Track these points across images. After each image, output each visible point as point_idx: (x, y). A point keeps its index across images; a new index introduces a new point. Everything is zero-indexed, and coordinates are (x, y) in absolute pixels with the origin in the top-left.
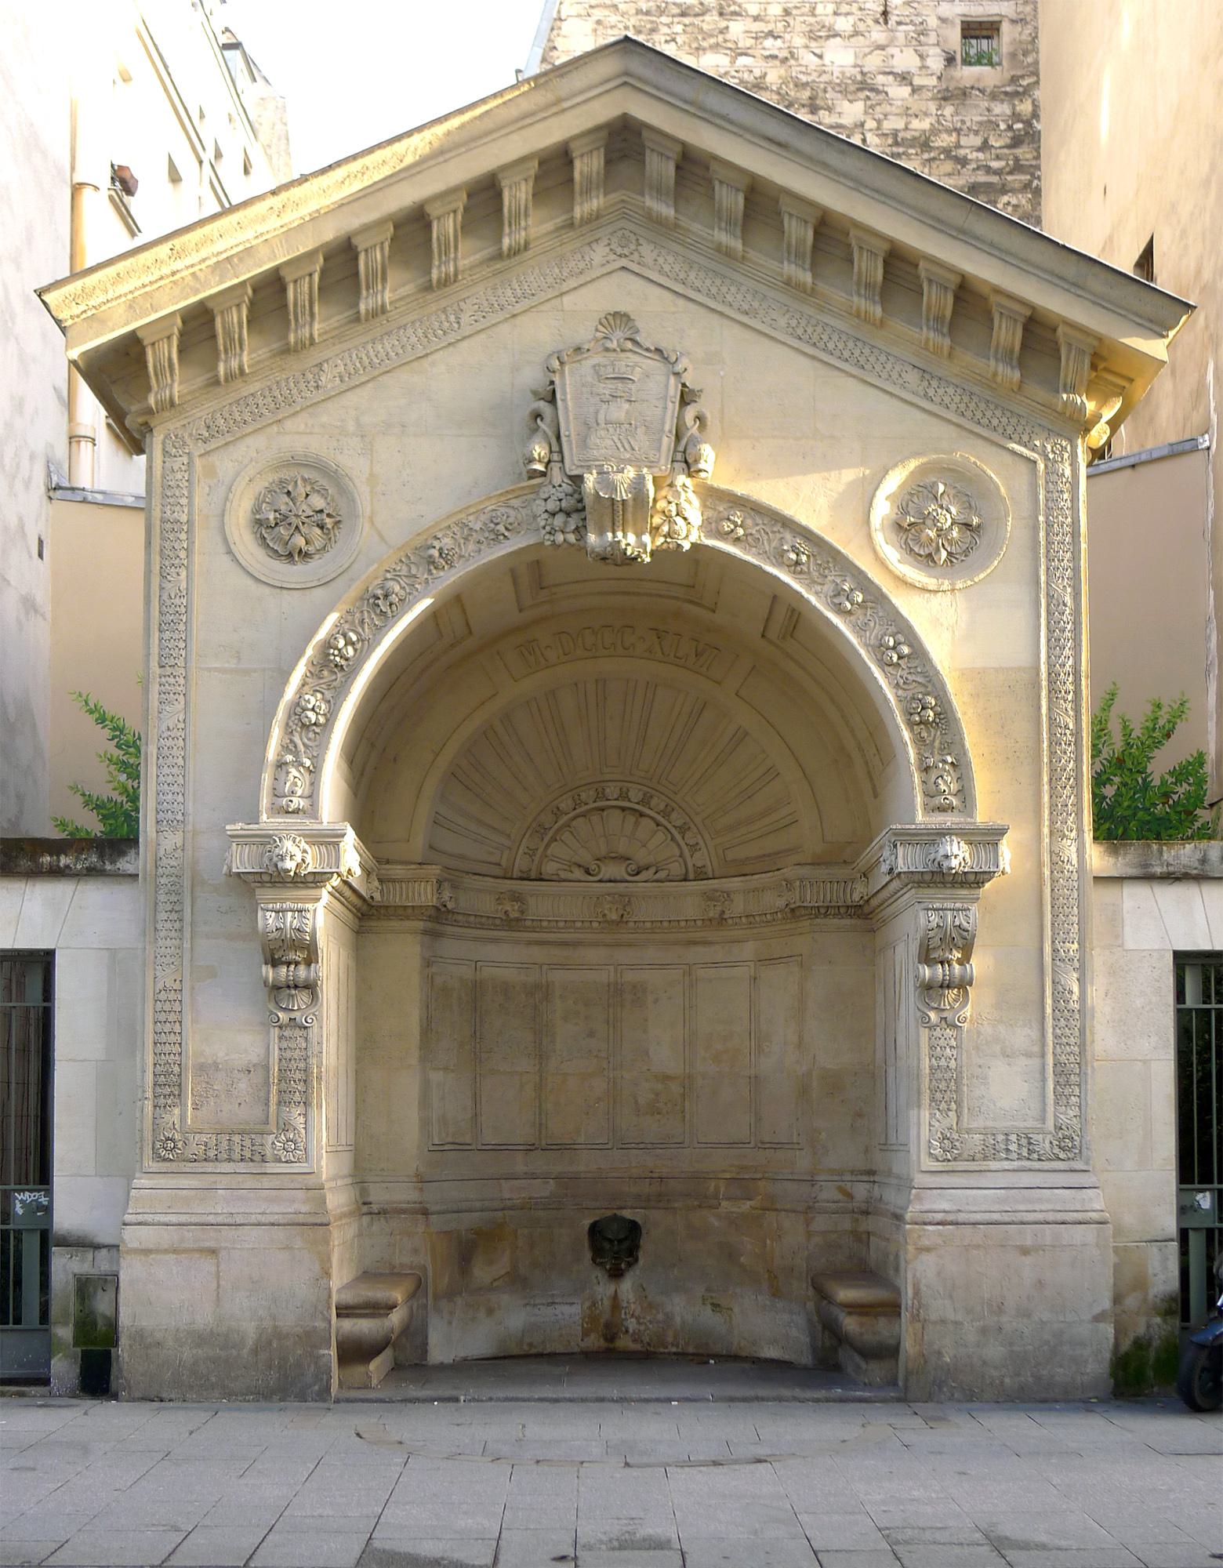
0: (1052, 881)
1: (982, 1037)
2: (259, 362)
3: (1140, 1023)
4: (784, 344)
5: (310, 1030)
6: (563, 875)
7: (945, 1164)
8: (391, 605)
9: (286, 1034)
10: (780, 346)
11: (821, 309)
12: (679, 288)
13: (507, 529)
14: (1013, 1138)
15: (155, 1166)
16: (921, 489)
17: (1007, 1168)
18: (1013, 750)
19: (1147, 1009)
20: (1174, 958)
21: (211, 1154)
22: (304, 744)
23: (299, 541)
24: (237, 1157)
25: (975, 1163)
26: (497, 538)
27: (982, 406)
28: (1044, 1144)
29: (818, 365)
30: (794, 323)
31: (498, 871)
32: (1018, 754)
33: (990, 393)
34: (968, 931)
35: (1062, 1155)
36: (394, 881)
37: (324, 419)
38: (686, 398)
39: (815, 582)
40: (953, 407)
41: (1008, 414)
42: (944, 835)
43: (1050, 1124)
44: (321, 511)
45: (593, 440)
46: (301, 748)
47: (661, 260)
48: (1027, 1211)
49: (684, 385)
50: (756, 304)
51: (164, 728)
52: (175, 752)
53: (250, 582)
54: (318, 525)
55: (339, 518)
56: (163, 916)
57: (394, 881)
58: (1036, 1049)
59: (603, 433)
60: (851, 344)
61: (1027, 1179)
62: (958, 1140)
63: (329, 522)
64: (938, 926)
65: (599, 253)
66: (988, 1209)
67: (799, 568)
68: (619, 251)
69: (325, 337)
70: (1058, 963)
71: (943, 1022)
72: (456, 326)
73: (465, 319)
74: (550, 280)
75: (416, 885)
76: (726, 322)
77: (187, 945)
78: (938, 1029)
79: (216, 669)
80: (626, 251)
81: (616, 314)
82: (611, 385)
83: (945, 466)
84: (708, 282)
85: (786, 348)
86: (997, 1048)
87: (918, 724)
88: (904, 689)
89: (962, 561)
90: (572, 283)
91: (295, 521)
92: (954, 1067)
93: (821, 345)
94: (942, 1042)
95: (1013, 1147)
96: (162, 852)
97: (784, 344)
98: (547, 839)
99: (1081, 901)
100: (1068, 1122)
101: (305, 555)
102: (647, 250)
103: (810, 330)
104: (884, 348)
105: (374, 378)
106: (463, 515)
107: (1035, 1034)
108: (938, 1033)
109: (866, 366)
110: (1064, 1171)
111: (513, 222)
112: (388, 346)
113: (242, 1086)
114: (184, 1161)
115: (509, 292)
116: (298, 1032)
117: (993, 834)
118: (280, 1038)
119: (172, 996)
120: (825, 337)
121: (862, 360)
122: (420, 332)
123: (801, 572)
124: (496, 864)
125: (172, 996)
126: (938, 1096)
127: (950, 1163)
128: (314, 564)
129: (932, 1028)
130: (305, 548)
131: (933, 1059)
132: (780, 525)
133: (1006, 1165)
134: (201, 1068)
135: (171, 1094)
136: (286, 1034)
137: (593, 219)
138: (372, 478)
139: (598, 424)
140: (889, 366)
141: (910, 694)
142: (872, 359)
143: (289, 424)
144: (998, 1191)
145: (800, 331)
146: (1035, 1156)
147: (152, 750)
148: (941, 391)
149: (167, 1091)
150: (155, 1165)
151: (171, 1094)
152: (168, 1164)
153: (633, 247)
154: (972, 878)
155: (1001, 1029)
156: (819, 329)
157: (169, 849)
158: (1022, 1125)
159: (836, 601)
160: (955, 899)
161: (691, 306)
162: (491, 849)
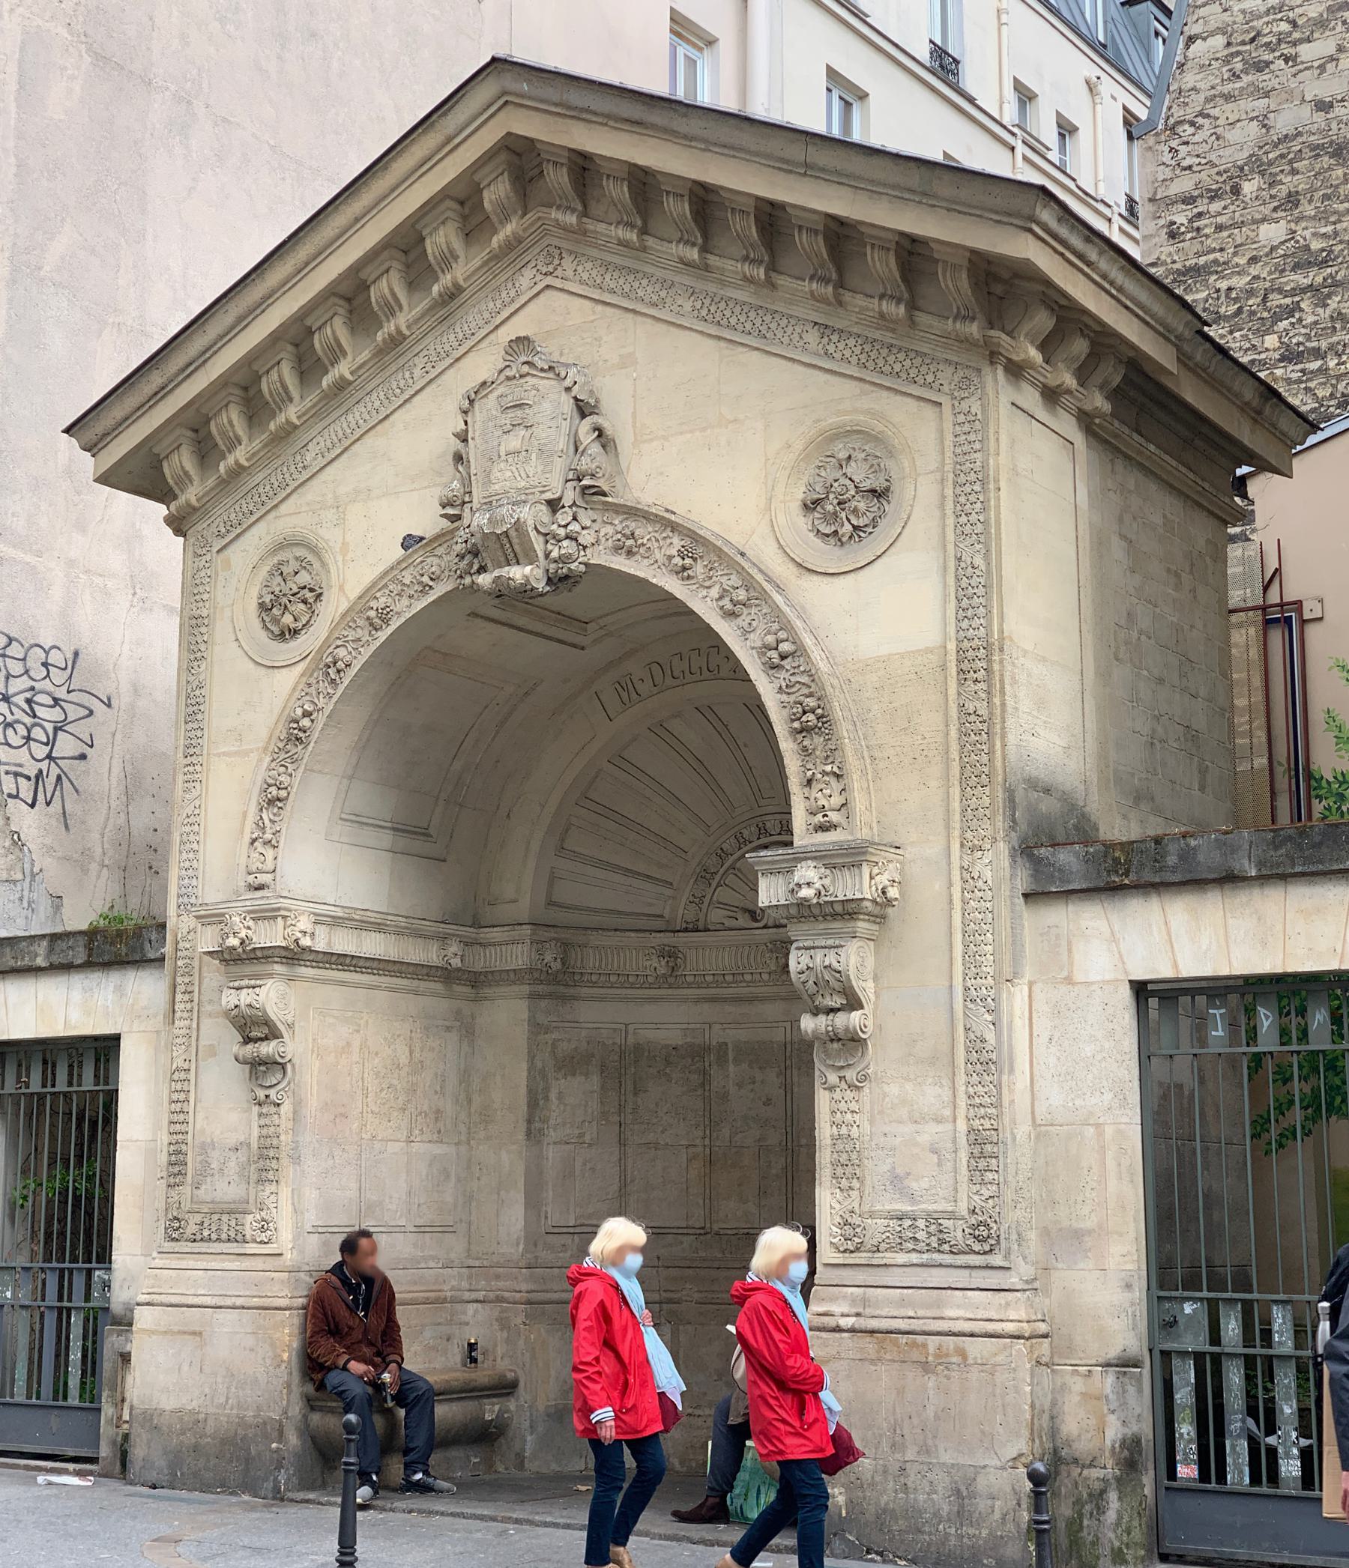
0: (965, 902)
1: (887, 1100)
2: (254, 455)
3: (1090, 1076)
4: (691, 329)
5: (282, 1107)
6: (729, 923)
7: (847, 1255)
8: (339, 671)
9: (264, 1110)
10: (687, 333)
11: (723, 283)
13: (432, 579)
14: (921, 1223)
15: (169, 1246)
16: (829, 459)
17: (915, 1261)
18: (921, 747)
19: (1099, 1057)
20: (96, 1038)
21: (206, 1233)
22: (270, 820)
23: (287, 619)
24: (224, 1236)
25: (880, 1255)
26: (425, 589)
27: (884, 352)
28: (958, 1233)
29: (723, 344)
30: (698, 304)
31: (658, 924)
32: (925, 753)
33: (891, 335)
34: (839, 972)
35: (977, 1247)
36: (494, 944)
38: (583, 409)
39: (702, 586)
40: (854, 360)
41: (912, 355)
42: (806, 859)
43: (963, 1208)
44: (305, 587)
45: (496, 474)
46: (267, 822)
47: (580, 269)
48: (934, 1318)
49: (576, 399)
50: (663, 294)
51: (185, 815)
52: (192, 837)
53: (251, 665)
54: (303, 601)
55: (320, 591)
56: (179, 997)
57: (494, 944)
58: (948, 1112)
59: (502, 465)
60: (752, 315)
61: (937, 1277)
62: (860, 1226)
63: (309, 595)
64: (808, 968)
65: (526, 278)
66: (890, 1314)
67: (685, 574)
68: (544, 270)
69: (305, 418)
70: (971, 1006)
71: (843, 1082)
72: (411, 381)
73: (417, 372)
74: (486, 315)
75: (520, 946)
76: (640, 319)
77: (194, 1026)
78: (838, 1090)
79: (224, 754)
80: (550, 268)
81: (518, 338)
82: (511, 414)
83: (849, 428)
84: (621, 281)
85: (693, 334)
87: (801, 732)
88: (789, 694)
89: (871, 533)
90: (505, 314)
91: (284, 600)
92: (856, 1136)
93: (724, 322)
94: (843, 1106)
95: (921, 1235)
96: (180, 936)
97: (691, 329)
98: (714, 884)
99: (996, 926)
100: (983, 1204)
101: (295, 633)
102: (568, 263)
103: (713, 309)
104: (785, 311)
105: (346, 449)
106: (396, 572)
107: (946, 1094)
108: (837, 1095)
109: (768, 335)
110: (980, 1267)
111: (444, 266)
112: (357, 414)
113: (232, 1164)
114: (186, 1240)
115: (452, 337)
116: (273, 1109)
117: (853, 854)
118: (260, 1115)
119: (183, 1075)
120: (728, 313)
121: (763, 329)
122: (382, 397)
123: (689, 577)
124: (659, 916)
125: (183, 1075)
126: (840, 1171)
127: (853, 1255)
128: (302, 638)
129: (831, 1089)
130: (292, 626)
131: (834, 1127)
132: (669, 529)
133: (915, 1258)
135: (180, 1173)
136: (264, 1110)
137: (511, 246)
139: (499, 456)
140: (789, 330)
141: (792, 698)
142: (773, 326)
143: (284, 508)
144: (905, 1291)
145: (704, 312)
146: (946, 1247)
147: (176, 837)
148: (841, 346)
149: (176, 1169)
150: (166, 1244)
151: (180, 1173)
152: (173, 1244)
153: (556, 262)
154: (838, 908)
156: (722, 305)
157: (185, 931)
158: (931, 1207)
159: (721, 603)
160: (827, 934)
161: (609, 310)
162: (649, 900)
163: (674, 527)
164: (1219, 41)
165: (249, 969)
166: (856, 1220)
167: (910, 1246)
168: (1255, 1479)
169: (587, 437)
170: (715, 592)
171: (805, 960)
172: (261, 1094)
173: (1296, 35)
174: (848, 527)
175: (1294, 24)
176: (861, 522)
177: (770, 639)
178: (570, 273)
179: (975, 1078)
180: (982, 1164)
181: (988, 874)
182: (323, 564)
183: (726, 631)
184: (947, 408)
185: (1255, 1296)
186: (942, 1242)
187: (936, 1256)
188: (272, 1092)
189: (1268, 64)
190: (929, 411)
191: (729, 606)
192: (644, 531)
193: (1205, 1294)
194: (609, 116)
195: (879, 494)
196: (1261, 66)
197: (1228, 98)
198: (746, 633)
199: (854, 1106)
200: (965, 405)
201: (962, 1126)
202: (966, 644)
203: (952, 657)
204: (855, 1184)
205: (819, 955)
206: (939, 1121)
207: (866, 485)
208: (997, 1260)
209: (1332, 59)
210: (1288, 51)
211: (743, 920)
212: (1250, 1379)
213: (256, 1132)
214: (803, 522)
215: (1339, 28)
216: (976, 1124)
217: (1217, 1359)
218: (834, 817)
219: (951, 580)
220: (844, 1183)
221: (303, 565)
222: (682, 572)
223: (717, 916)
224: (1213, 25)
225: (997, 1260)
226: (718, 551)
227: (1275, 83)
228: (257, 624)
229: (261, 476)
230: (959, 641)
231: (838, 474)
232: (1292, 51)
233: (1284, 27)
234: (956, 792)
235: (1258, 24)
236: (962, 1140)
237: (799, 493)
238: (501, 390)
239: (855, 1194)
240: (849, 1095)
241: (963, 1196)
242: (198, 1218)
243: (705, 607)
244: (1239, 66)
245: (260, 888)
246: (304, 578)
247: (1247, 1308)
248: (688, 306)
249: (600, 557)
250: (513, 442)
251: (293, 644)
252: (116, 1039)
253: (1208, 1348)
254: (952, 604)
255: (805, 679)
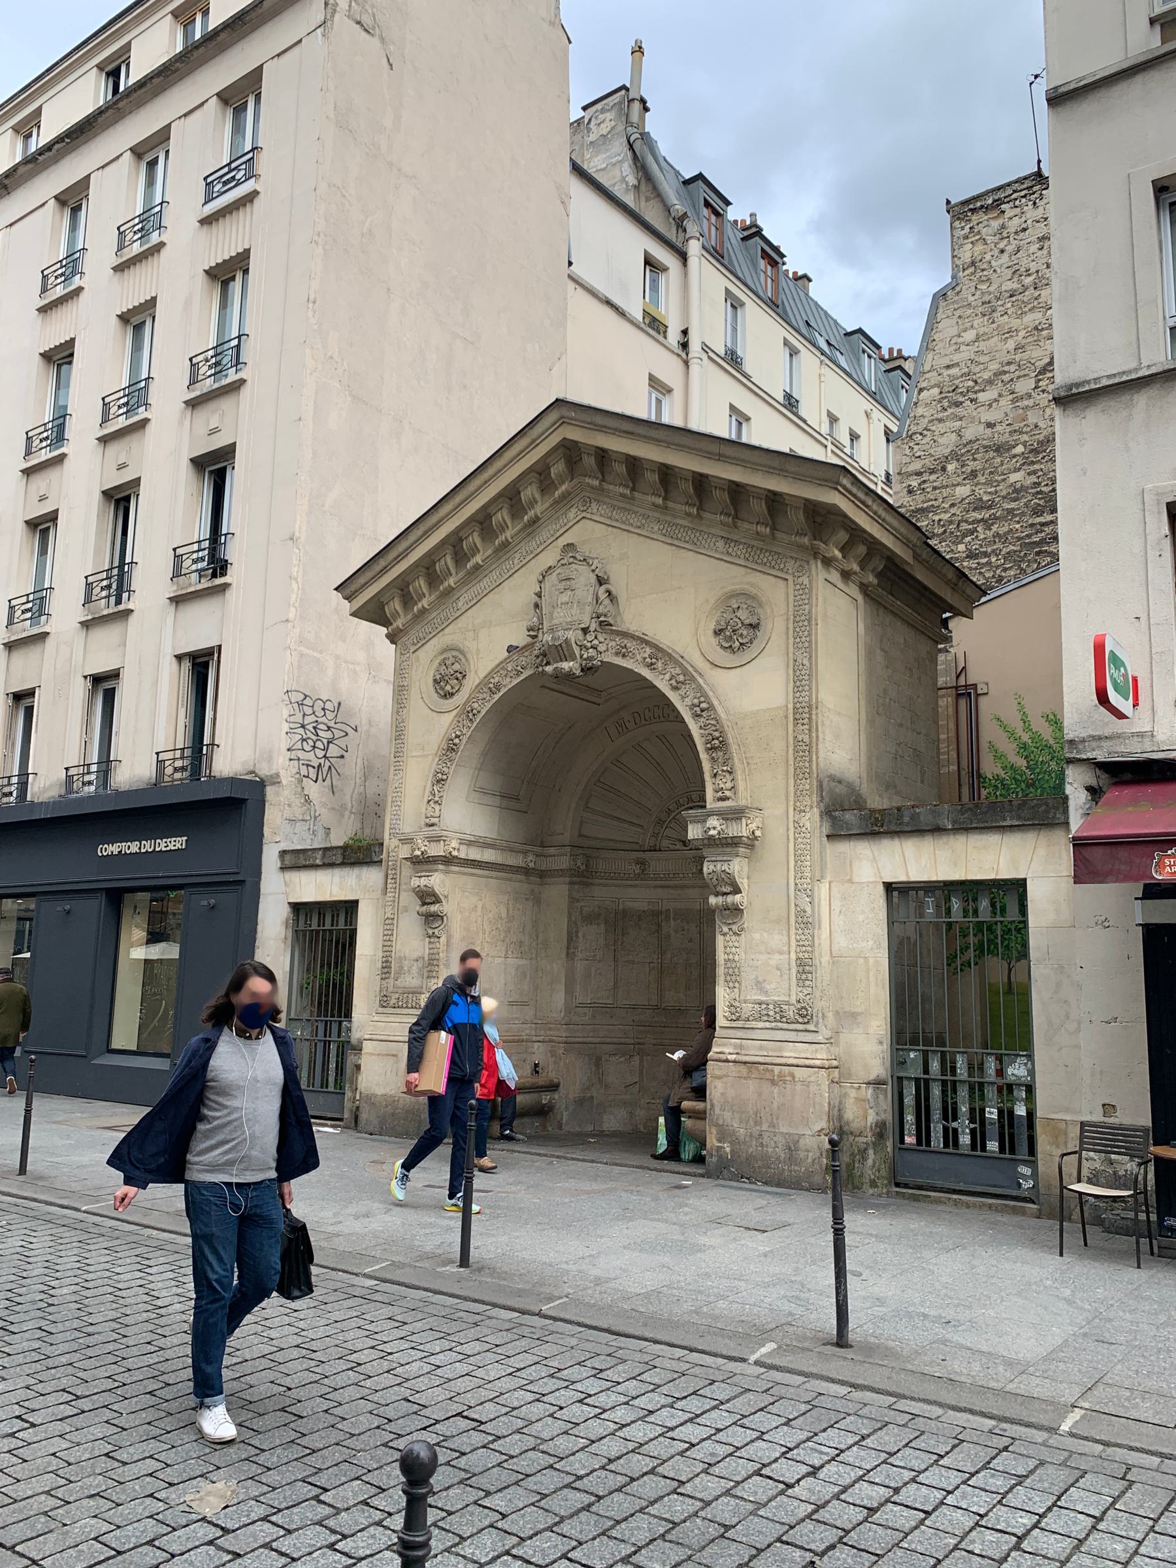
0: (796, 839)
6: (672, 847)
11: (674, 516)
12: (608, 522)
14: (771, 1007)
15: (381, 1010)
20: (346, 902)
23: (448, 688)
26: (519, 673)
28: (790, 1013)
31: (637, 847)
35: (800, 1020)
37: (460, 625)
38: (601, 581)
43: (793, 1000)
45: (555, 614)
58: (785, 949)
61: (780, 1035)
65: (572, 514)
73: (516, 561)
82: (564, 583)
86: (763, 948)
90: (561, 531)
94: (730, 944)
95: (771, 1013)
102: (594, 506)
108: (728, 938)
113: (414, 968)
128: (455, 697)
129: (725, 935)
133: (767, 1025)
134: (400, 958)
137: (564, 496)
138: (478, 650)
147: (390, 799)
154: (729, 841)
155: (765, 935)
160: (724, 854)
163: (647, 643)
164: (936, 391)
165: (425, 867)
166: (737, 1004)
167: (765, 1018)
168: (946, 1145)
169: (603, 596)
170: (667, 677)
171: (712, 867)
172: (430, 932)
173: (977, 388)
174: (737, 644)
175: (976, 382)
176: (744, 641)
177: (696, 701)
178: (595, 511)
179: (800, 931)
180: (804, 977)
181: (808, 825)
182: (467, 660)
183: (673, 697)
184: (790, 582)
185: (947, 1049)
186: (782, 1017)
187: (779, 1024)
188: (436, 931)
189: (961, 403)
190: (781, 583)
191: (675, 684)
192: (631, 645)
193: (921, 1047)
194: (616, 430)
195: (754, 627)
196: (958, 404)
197: (940, 420)
198: (683, 698)
199: (736, 944)
200: (800, 580)
201: (793, 956)
202: (798, 705)
203: (791, 711)
204: (737, 985)
205: (719, 865)
206: (781, 953)
207: (747, 622)
208: (811, 1027)
209: (996, 400)
210: (973, 396)
211: (679, 846)
212: (944, 1092)
213: (427, 951)
214: (714, 641)
215: (1000, 384)
216: (801, 955)
217: (927, 1081)
218: (728, 793)
219: (791, 672)
220: (731, 985)
221: (457, 660)
222: (651, 666)
223: (665, 843)
224: (933, 382)
225: (811, 1027)
226: (670, 655)
227: (965, 413)
228: (432, 690)
229: (435, 614)
230: (795, 704)
231: (733, 616)
232: (974, 396)
233: (971, 383)
234: (792, 781)
235: (957, 382)
236: (793, 963)
237: (712, 626)
238: (558, 571)
239: (736, 990)
240: (734, 938)
241: (793, 993)
242: (397, 996)
243: (662, 685)
244: (946, 404)
245: (432, 825)
246: (457, 667)
247: (943, 1054)
248: (656, 528)
249: (609, 658)
250: (564, 598)
251: (451, 700)
252: (356, 902)
253: (922, 1076)
254: (792, 683)
255: (713, 722)
